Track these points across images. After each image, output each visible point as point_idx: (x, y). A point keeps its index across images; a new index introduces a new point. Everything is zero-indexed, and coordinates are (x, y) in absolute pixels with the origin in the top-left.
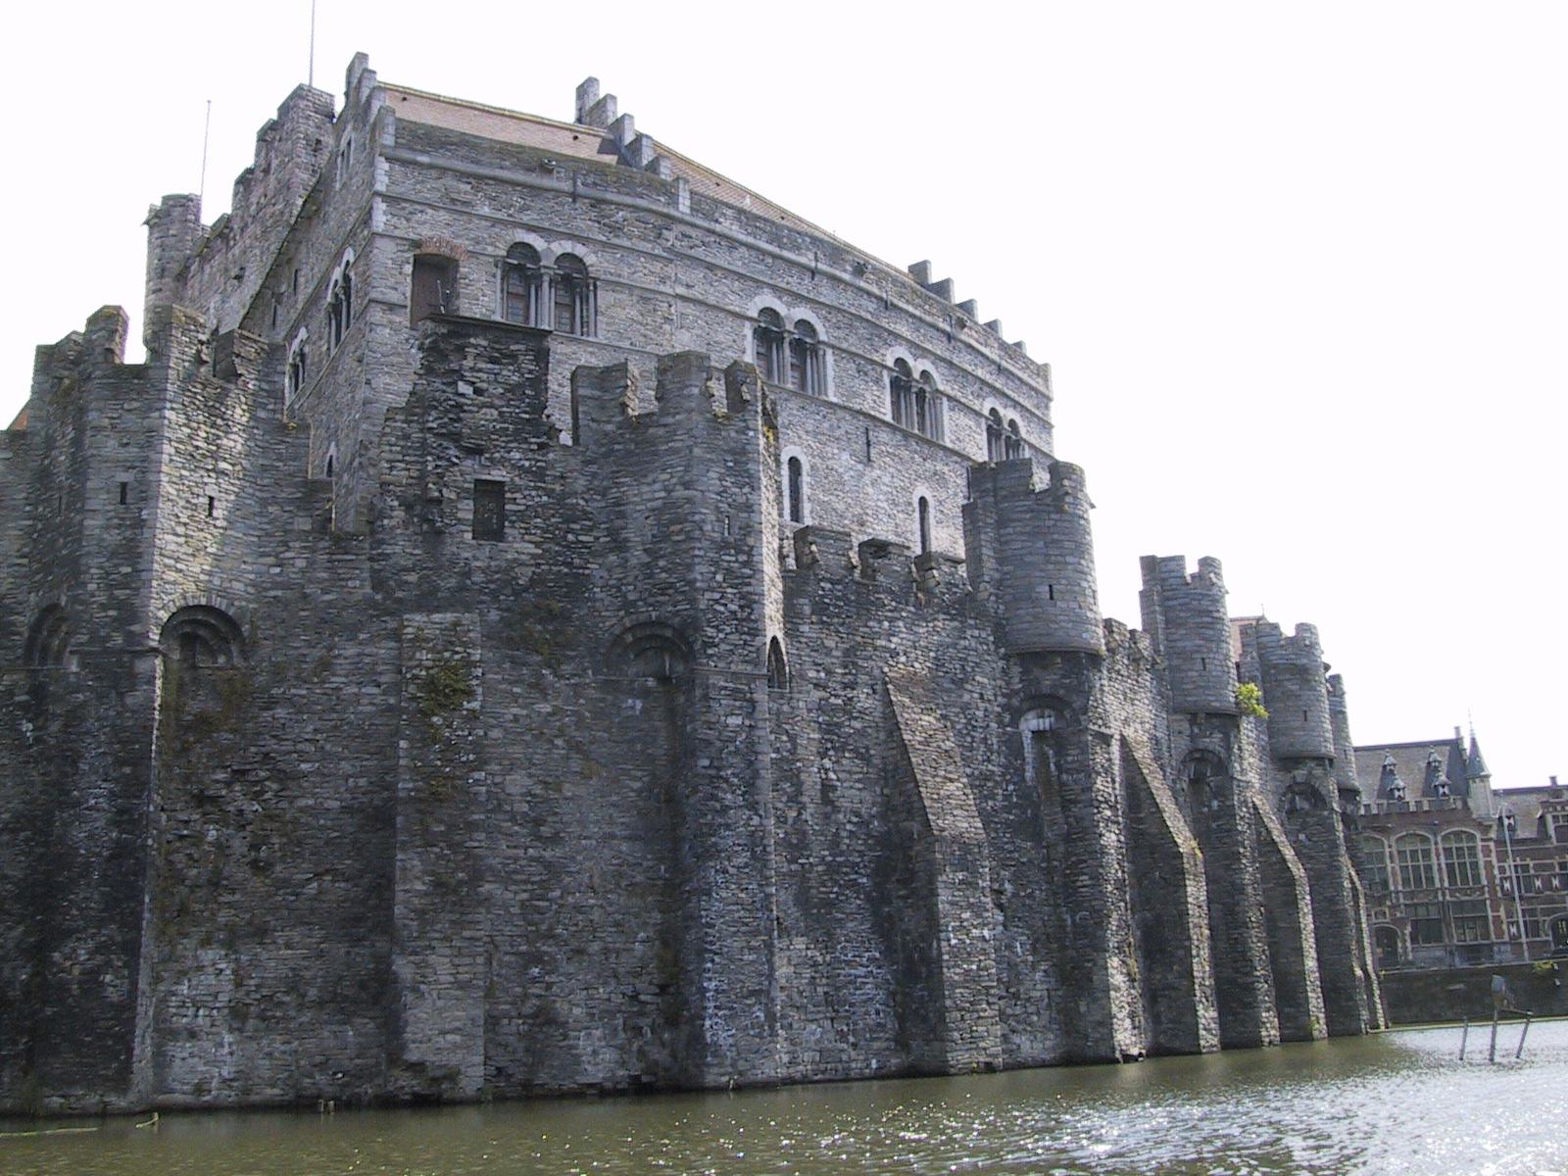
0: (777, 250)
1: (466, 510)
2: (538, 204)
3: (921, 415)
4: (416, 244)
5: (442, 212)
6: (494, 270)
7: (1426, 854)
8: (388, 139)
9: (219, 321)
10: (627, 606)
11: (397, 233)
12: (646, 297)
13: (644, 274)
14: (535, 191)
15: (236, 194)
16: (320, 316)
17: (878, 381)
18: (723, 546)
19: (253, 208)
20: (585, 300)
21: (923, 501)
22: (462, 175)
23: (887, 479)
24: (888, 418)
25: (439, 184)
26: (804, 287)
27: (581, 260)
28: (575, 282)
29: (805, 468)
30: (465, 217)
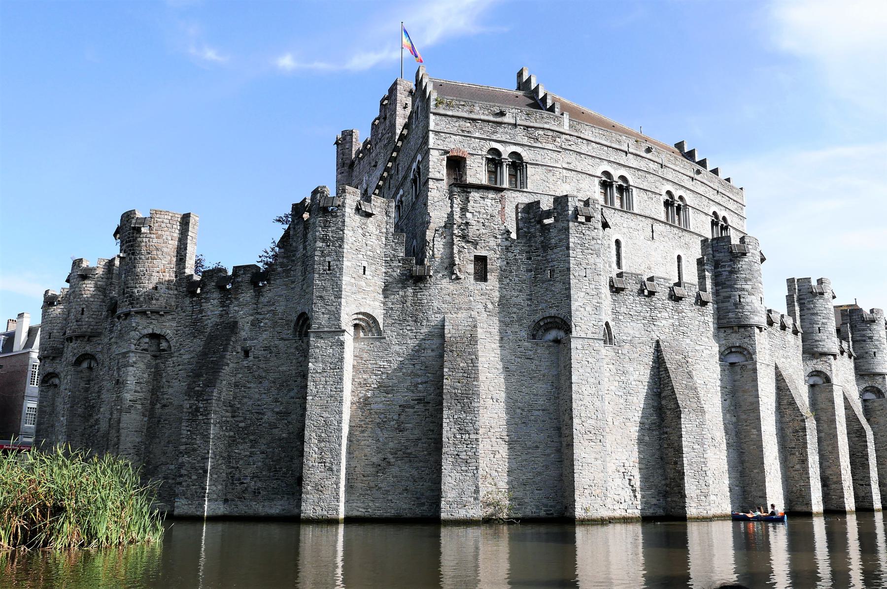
0: (609, 144)
1: (471, 268)
2: (501, 130)
4: (446, 152)
5: (458, 137)
6: (481, 161)
9: (368, 185)
11: (439, 147)
13: (548, 158)
15: (372, 129)
16: (408, 184)
19: (380, 135)
20: (522, 171)
21: (679, 258)
23: (662, 247)
24: (663, 219)
25: (457, 124)
26: (622, 159)
27: (520, 155)
30: (468, 138)
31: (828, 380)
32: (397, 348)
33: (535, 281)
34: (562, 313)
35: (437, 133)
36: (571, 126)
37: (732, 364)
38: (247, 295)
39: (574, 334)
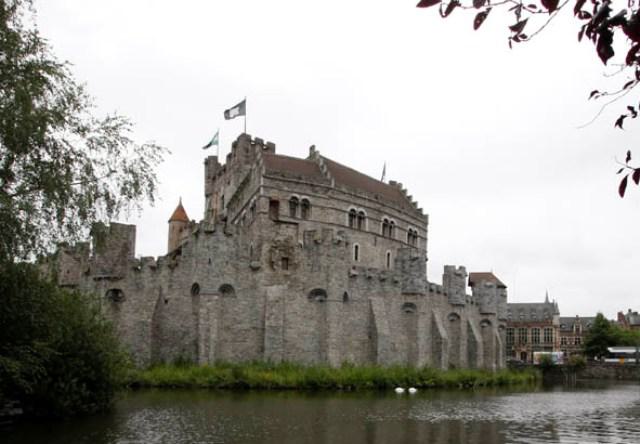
1: (280, 263)
2: (299, 186)
4: (270, 198)
8: (263, 172)
12: (322, 208)
13: (322, 203)
22: (280, 180)
24: (381, 233)
26: (359, 201)
28: (306, 205)
31: (459, 317)
32: (244, 303)
33: (312, 271)
34: (324, 287)
35: (264, 187)
36: (335, 185)
37: (408, 312)
38: (165, 272)
39: (329, 298)
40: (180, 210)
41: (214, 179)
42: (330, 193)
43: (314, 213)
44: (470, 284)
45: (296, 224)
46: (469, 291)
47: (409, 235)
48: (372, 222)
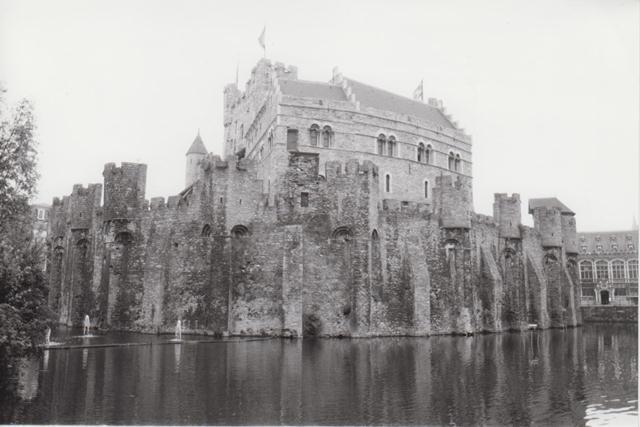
1: (299, 200)
3: (428, 157)
7: (622, 267)
10: (338, 222)
14: (318, 109)
17: (413, 150)
18: (361, 208)
28: (328, 132)
29: (391, 176)
40: (197, 147)
41: (233, 107)
42: (355, 118)
43: (338, 140)
44: (531, 211)
45: (317, 155)
46: (528, 221)
47: (451, 159)
48: (406, 147)
